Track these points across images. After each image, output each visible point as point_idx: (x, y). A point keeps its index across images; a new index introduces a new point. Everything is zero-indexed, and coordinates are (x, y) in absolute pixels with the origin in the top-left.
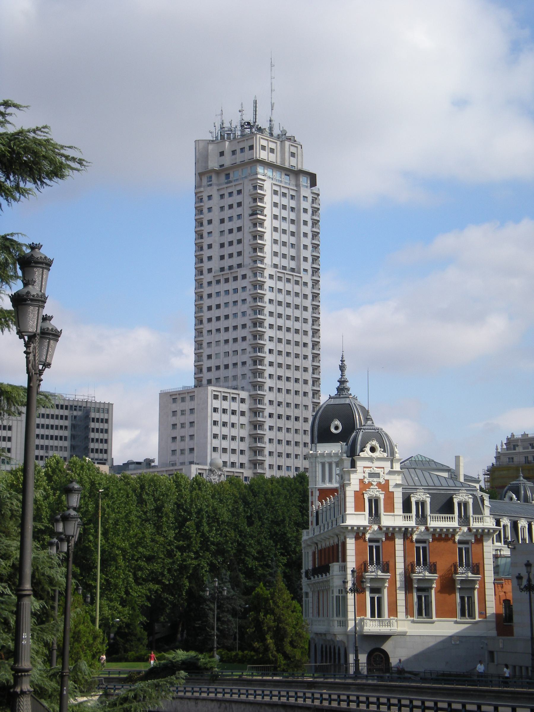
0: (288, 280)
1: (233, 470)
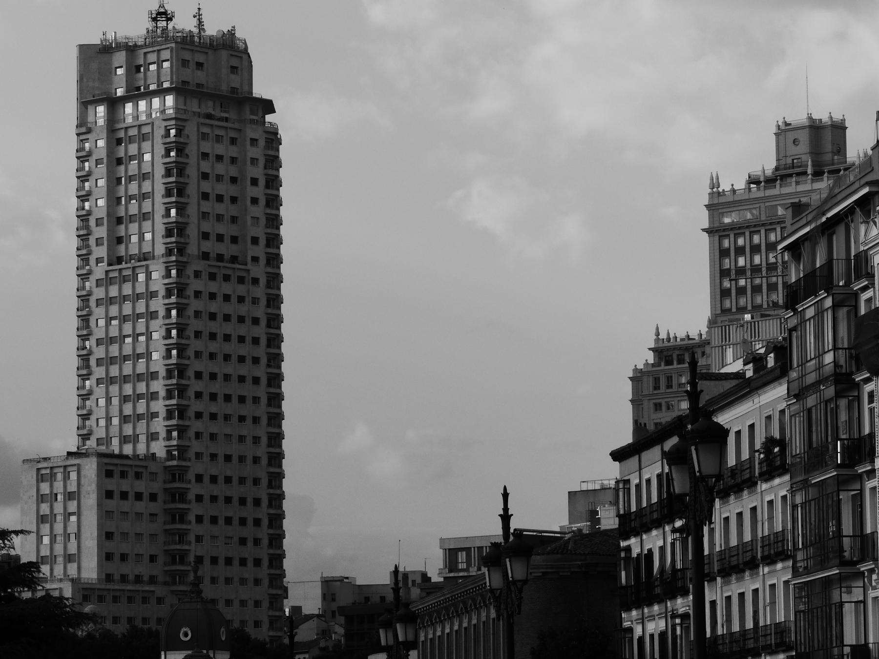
0: (227, 278)
1: (138, 587)
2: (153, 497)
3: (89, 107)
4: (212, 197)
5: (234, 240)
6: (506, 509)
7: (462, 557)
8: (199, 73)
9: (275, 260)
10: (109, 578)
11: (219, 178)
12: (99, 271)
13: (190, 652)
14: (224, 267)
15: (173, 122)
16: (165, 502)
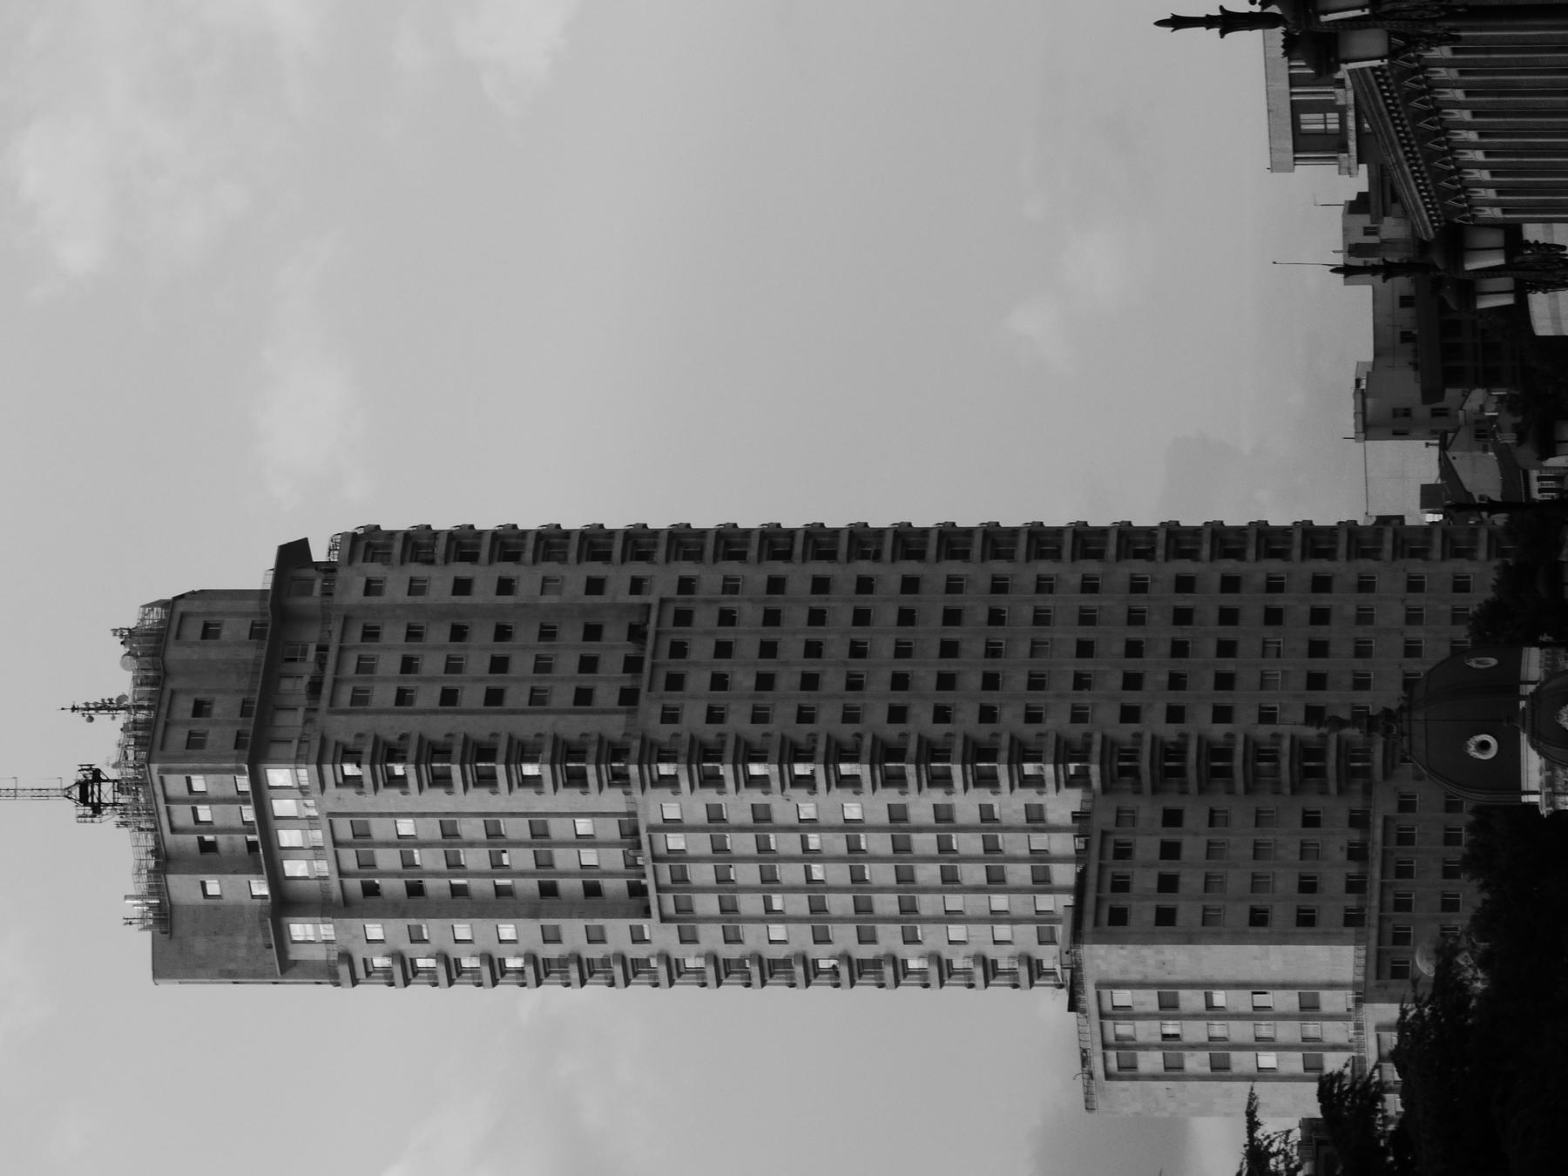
0: (679, 650)
1: (1376, 852)
2: (1172, 818)
3: (292, 957)
4: (496, 681)
5: (593, 632)
6: (1208, 22)
7: (1311, 122)
8: (217, 710)
9: (638, 542)
10: (1353, 919)
11: (453, 666)
12: (662, 936)
13: (1524, 737)
14: (654, 655)
15: (328, 768)
16: (1184, 792)
